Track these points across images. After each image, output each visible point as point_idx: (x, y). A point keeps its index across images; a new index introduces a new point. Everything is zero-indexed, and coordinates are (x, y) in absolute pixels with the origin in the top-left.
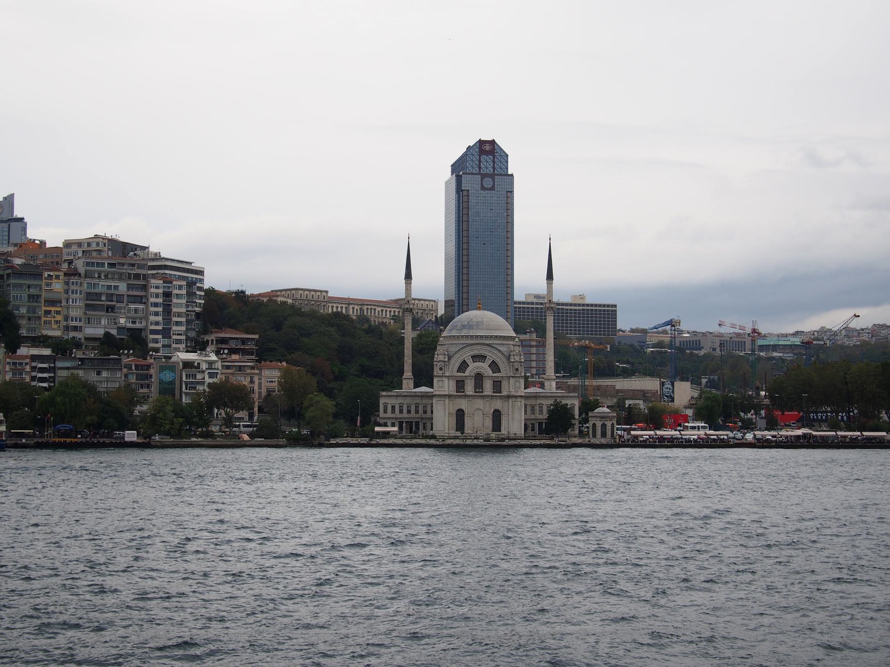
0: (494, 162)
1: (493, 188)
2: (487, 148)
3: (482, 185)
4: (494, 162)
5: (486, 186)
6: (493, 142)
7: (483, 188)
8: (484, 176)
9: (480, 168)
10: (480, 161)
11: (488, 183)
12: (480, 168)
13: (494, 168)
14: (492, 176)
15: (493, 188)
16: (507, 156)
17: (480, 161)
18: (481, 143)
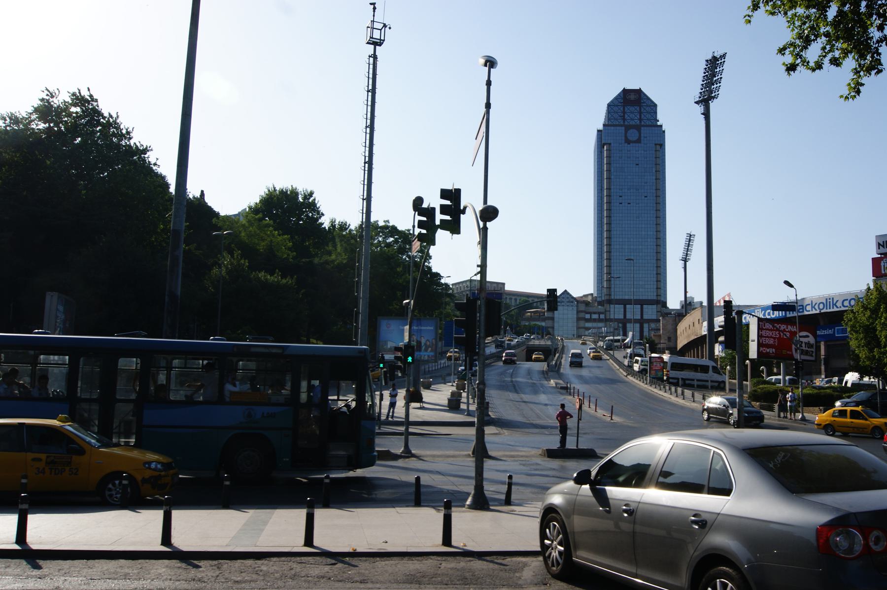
0: (640, 113)
1: (639, 141)
2: (632, 97)
3: (626, 136)
4: (640, 113)
5: (630, 138)
6: (639, 92)
7: (628, 142)
8: (628, 128)
9: (624, 120)
10: (624, 112)
11: (633, 135)
12: (624, 120)
13: (640, 120)
14: (638, 128)
15: (639, 141)
16: (655, 106)
17: (624, 112)
18: (625, 92)
